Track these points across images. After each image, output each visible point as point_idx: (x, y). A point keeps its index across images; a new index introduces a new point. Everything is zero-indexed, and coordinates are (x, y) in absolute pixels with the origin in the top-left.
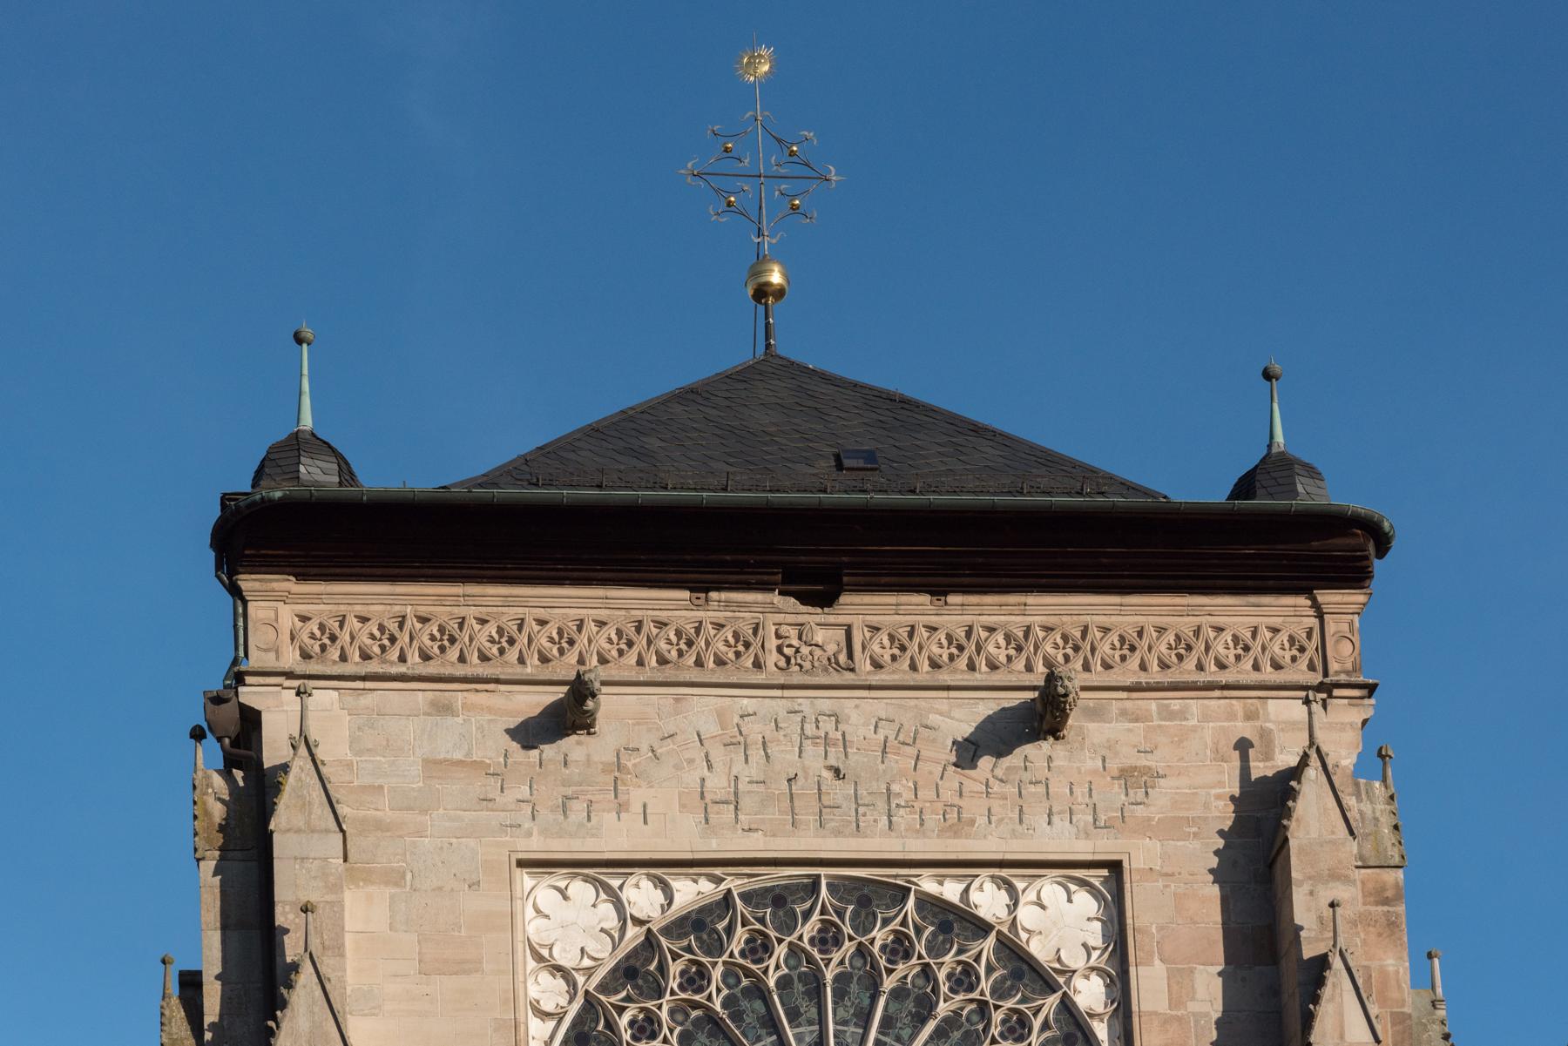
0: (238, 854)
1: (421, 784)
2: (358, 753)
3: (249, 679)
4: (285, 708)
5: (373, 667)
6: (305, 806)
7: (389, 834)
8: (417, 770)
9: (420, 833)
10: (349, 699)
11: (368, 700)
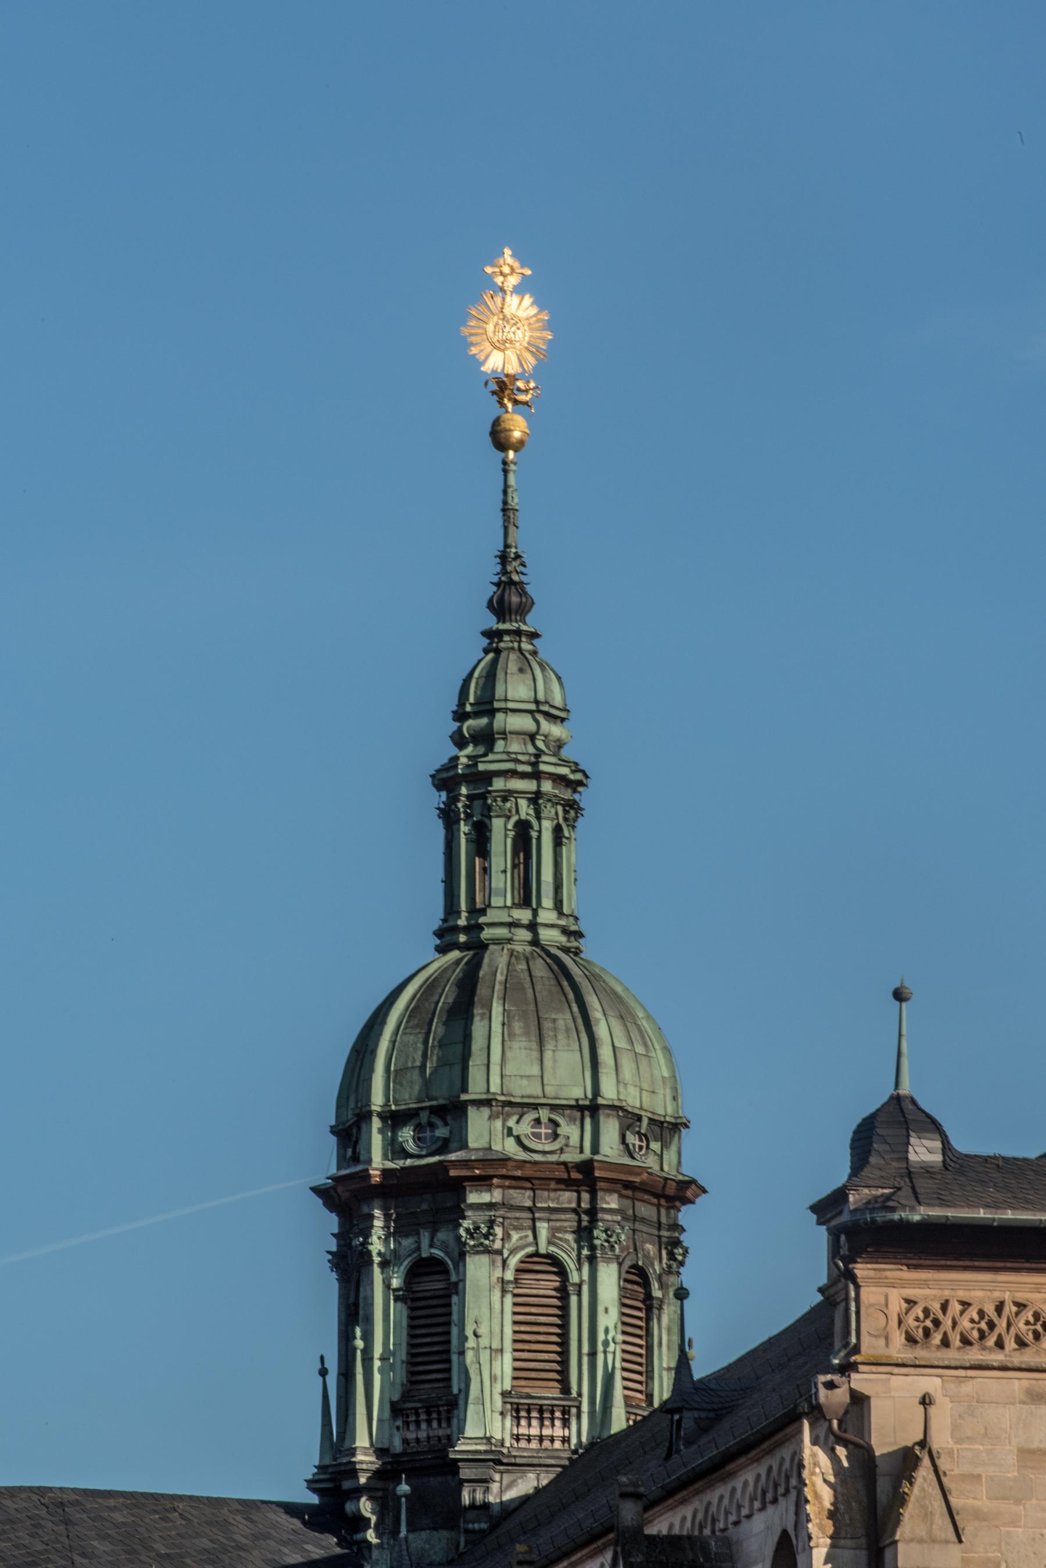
0: (849, 1543)
1: (1016, 1474)
2: (959, 1441)
3: (861, 1368)
4: (893, 1394)
5: (974, 1355)
6: (927, 1516)
7: (986, 1523)
8: (1012, 1459)
9: (1014, 1523)
10: (951, 1386)
11: (968, 1388)
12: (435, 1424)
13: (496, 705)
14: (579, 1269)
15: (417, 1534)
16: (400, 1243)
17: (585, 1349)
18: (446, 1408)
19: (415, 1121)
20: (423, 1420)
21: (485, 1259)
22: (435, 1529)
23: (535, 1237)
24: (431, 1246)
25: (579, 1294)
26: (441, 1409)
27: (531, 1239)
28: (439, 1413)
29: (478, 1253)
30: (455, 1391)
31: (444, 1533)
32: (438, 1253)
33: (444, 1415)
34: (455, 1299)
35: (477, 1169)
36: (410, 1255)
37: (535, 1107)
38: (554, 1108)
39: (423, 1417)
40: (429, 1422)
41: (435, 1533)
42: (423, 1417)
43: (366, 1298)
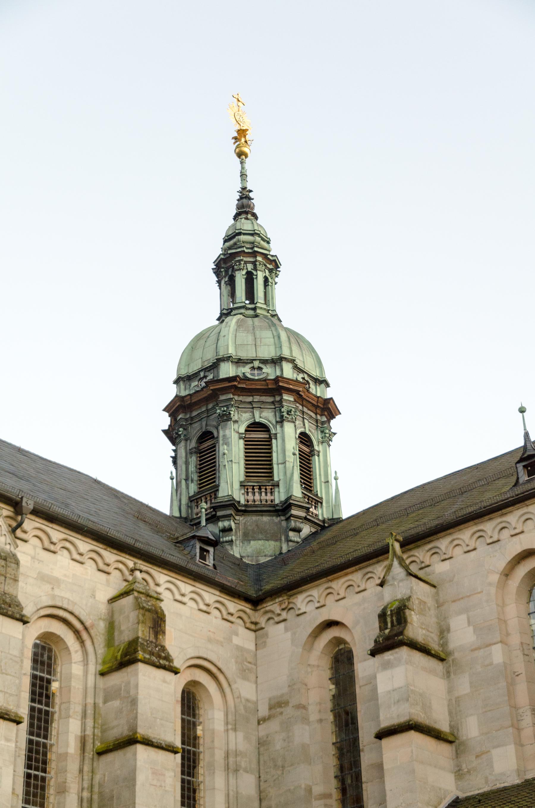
12: (263, 494)
13: (256, 231)
14: (318, 445)
15: (256, 542)
16: (241, 415)
17: (323, 480)
18: (270, 487)
19: (251, 365)
20: (257, 492)
21: (292, 425)
22: (268, 540)
23: (304, 425)
24: (260, 417)
25: (318, 456)
26: (267, 487)
27: (302, 425)
28: (266, 489)
29: (289, 421)
30: (276, 479)
31: (272, 543)
32: (263, 421)
33: (269, 490)
34: (274, 441)
35: (291, 385)
36: (248, 420)
37: (303, 372)
38: (309, 375)
39: (256, 490)
40: (260, 493)
41: (267, 542)
42: (256, 490)
43: (224, 436)
